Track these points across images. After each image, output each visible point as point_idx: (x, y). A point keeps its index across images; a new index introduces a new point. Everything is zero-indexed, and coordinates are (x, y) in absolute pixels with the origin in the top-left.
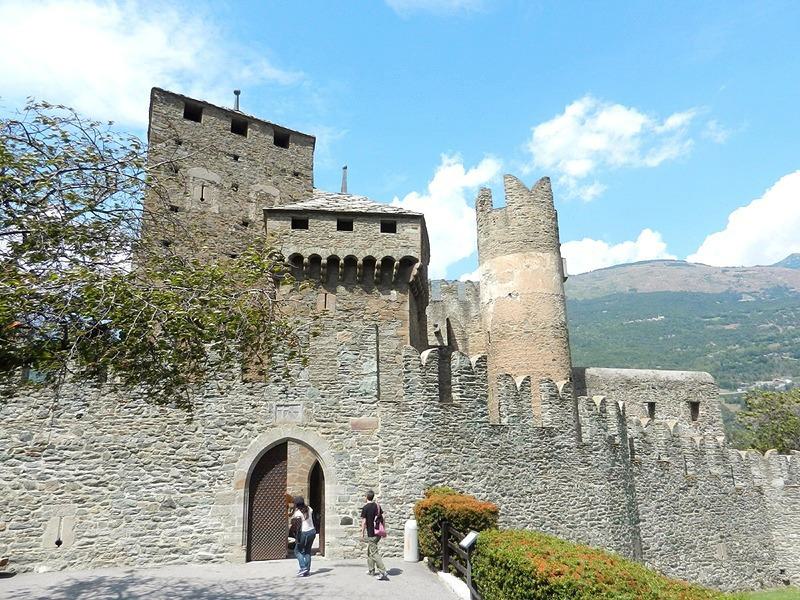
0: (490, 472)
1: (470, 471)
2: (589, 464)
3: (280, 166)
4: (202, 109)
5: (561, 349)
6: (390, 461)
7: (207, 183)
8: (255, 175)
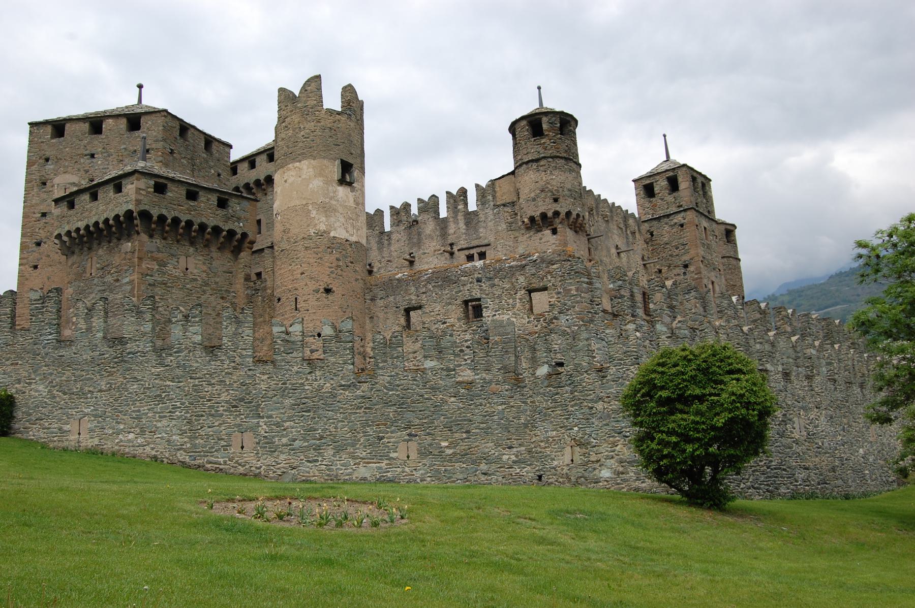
0: (53, 376)
1: (33, 376)
2: (167, 366)
3: (131, 148)
4: (65, 124)
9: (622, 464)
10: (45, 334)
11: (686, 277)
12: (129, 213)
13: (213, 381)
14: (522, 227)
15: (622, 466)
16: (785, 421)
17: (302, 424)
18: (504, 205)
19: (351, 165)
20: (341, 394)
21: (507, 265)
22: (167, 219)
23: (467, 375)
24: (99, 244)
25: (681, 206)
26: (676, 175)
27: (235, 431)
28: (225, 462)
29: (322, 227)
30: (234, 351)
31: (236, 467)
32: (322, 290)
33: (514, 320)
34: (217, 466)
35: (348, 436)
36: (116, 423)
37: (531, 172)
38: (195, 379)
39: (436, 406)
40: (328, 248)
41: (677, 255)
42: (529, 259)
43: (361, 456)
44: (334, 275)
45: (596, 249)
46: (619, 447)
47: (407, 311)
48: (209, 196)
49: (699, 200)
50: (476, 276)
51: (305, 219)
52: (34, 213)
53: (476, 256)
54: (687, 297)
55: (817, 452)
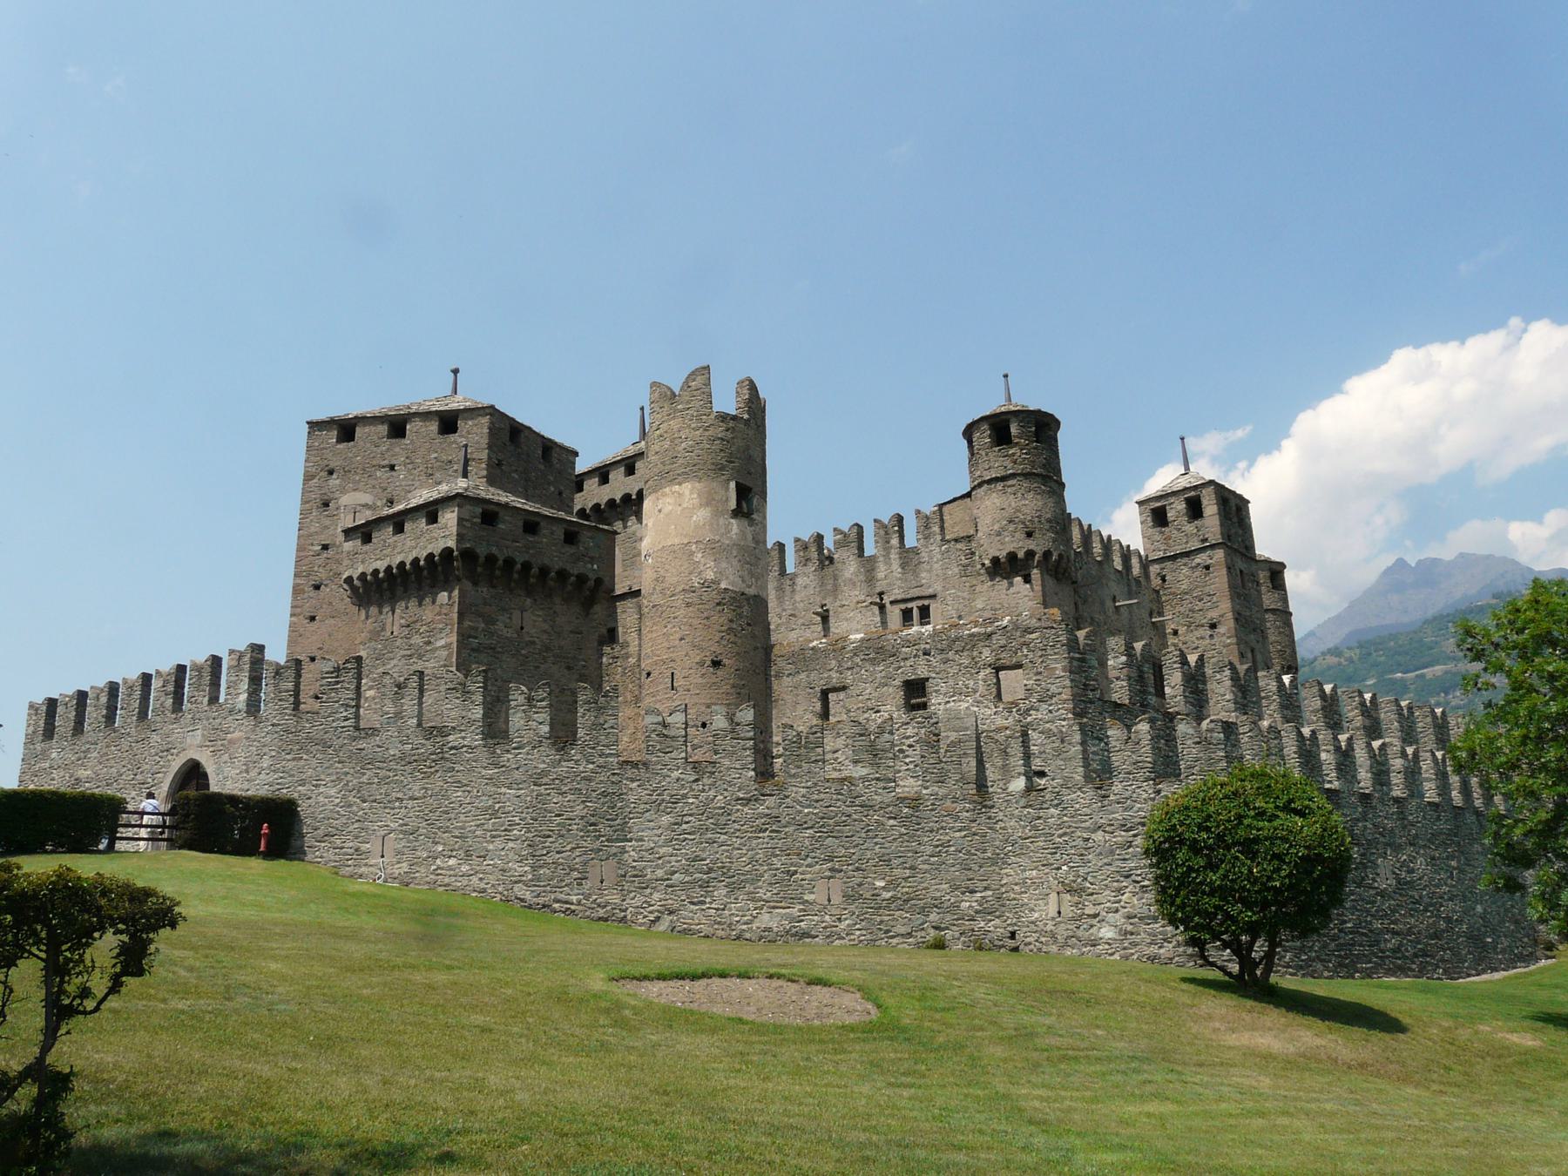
0: (349, 777)
1: (323, 777)
2: (502, 766)
5: (695, 622)
6: (247, 771)
7: (358, 508)
8: (413, 480)
9: (1131, 921)
10: (338, 719)
11: (1213, 642)
12: (447, 552)
13: (564, 789)
14: (982, 571)
15: (1131, 924)
16: (1364, 864)
17: (683, 851)
18: (956, 540)
19: (750, 490)
20: (738, 810)
21: (967, 632)
22: (497, 560)
23: (909, 785)
24: (405, 591)
25: (1206, 540)
26: (1199, 496)
27: (592, 859)
28: (579, 903)
29: (710, 575)
30: (594, 748)
31: (593, 909)
32: (708, 663)
33: (976, 709)
34: (568, 906)
35: (746, 869)
36: (433, 842)
37: (994, 495)
38: (540, 785)
39: (868, 831)
40: (718, 604)
41: (1200, 610)
42: (996, 624)
43: (765, 897)
44: (725, 643)
45: (1085, 602)
46: (1126, 895)
47: (825, 694)
48: (554, 528)
49: (1233, 531)
50: (923, 646)
51: (686, 565)
52: (312, 545)
53: (916, 613)
54: (1218, 676)
55: (1411, 909)
